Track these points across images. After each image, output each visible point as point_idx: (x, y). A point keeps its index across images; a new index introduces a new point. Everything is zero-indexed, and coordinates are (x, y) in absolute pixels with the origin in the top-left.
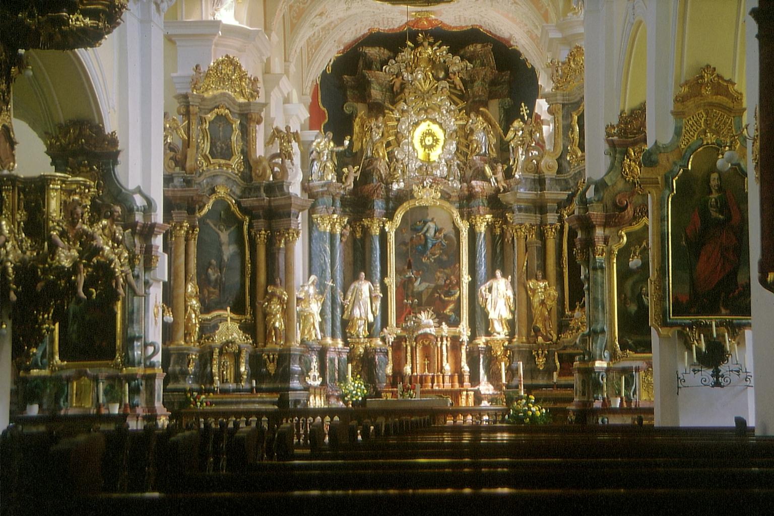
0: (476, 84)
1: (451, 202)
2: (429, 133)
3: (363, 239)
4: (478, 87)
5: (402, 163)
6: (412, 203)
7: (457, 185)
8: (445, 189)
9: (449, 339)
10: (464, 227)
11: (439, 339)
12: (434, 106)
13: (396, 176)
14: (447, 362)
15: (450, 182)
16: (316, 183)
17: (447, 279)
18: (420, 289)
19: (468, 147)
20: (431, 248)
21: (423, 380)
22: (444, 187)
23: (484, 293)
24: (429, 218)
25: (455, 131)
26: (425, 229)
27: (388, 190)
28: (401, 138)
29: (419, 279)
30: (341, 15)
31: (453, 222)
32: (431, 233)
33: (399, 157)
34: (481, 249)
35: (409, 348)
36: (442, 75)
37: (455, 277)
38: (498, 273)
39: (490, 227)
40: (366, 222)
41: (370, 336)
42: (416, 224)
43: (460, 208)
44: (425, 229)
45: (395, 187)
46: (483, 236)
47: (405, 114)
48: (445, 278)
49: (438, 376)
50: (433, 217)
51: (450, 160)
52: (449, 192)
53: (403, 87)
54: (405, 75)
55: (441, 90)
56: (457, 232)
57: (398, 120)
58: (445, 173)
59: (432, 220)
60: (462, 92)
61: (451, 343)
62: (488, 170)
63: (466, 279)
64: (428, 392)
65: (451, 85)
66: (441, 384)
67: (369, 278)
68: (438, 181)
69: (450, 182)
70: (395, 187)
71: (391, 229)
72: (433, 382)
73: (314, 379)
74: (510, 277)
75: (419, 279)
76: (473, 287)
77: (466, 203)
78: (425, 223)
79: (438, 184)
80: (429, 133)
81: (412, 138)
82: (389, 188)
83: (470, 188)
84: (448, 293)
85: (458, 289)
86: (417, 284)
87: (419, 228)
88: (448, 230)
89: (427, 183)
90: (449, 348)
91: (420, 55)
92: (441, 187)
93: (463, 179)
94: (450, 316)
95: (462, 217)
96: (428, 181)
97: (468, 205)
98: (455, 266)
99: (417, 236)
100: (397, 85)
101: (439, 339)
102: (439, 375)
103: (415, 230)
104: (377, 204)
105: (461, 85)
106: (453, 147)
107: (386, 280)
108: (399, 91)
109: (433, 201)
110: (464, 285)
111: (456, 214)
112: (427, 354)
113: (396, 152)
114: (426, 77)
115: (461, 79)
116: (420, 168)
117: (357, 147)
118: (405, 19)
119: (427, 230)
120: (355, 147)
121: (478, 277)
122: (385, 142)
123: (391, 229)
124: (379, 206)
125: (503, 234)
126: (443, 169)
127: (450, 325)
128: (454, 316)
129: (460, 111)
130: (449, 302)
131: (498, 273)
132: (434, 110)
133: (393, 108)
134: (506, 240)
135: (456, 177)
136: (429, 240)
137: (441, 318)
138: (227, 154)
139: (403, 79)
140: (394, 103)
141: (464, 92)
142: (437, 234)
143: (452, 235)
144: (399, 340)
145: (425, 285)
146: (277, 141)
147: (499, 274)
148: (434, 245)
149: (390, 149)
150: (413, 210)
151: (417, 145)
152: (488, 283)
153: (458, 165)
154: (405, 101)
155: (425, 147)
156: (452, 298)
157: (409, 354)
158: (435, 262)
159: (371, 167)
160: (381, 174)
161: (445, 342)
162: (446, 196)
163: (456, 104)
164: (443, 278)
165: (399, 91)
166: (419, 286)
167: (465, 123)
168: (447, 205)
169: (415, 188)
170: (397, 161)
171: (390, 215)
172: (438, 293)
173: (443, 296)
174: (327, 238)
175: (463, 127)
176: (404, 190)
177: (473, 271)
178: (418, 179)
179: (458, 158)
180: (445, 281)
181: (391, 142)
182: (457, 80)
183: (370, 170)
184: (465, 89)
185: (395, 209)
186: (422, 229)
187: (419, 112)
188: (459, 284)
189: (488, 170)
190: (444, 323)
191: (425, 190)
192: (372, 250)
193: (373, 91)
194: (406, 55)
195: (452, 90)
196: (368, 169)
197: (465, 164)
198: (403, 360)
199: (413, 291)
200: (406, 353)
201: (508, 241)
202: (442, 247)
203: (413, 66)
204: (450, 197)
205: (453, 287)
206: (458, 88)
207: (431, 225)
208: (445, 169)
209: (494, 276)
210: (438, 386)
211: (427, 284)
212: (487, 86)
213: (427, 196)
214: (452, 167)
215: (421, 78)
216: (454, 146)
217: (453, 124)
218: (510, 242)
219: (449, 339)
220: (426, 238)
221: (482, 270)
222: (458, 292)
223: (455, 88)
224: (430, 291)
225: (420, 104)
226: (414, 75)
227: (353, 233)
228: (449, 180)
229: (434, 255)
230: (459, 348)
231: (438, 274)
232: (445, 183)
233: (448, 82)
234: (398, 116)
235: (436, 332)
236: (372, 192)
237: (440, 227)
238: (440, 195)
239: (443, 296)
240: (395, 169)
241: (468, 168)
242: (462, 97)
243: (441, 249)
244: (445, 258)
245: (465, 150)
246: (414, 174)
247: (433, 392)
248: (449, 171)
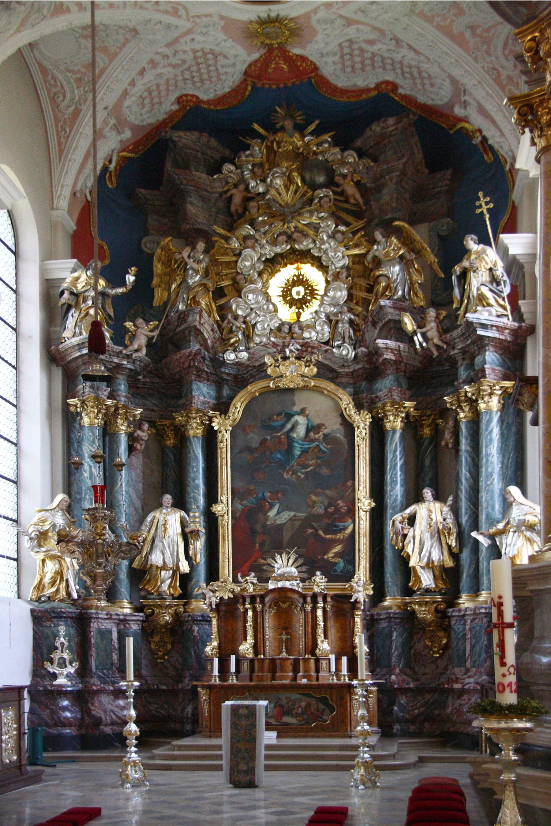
0: (385, 191)
1: (338, 384)
2: (299, 281)
4: (388, 194)
5: (244, 322)
6: (261, 384)
7: (347, 352)
8: (326, 362)
9: (329, 599)
11: (309, 599)
12: (305, 228)
13: (232, 341)
14: (326, 637)
15: (334, 350)
17: (330, 505)
18: (278, 522)
19: (370, 289)
20: (300, 456)
21: (274, 666)
22: (325, 358)
23: (399, 526)
24: (296, 408)
25: (347, 268)
26: (289, 426)
27: (218, 363)
28: (242, 282)
29: (277, 507)
31: (342, 415)
32: (301, 431)
33: (240, 312)
34: (395, 456)
35: (250, 613)
36: (321, 179)
37: (344, 502)
38: (428, 493)
42: (271, 419)
44: (289, 426)
46: (398, 435)
47: (249, 243)
48: (326, 504)
49: (306, 660)
50: (302, 406)
51: (336, 315)
52: (334, 366)
54: (252, 184)
55: (319, 202)
56: (349, 428)
57: (240, 254)
58: (327, 336)
59: (302, 412)
60: (360, 207)
61: (332, 606)
63: (364, 503)
64: (284, 687)
65: (338, 198)
66: (313, 674)
68: (313, 348)
69: (334, 350)
70: (230, 356)
71: (223, 426)
72: (296, 670)
73: (62, 664)
74: (451, 498)
75: (277, 507)
76: (378, 516)
77: (363, 378)
78: (289, 416)
79: (313, 353)
80: (299, 281)
81: (265, 285)
82: (218, 360)
84: (333, 529)
85: (350, 521)
86: (272, 513)
87: (276, 424)
88: (333, 426)
89: (291, 351)
90: (330, 614)
91: (279, 147)
94: (335, 564)
95: (359, 407)
96: (293, 348)
97: (371, 388)
98: (344, 484)
99: (272, 437)
100: (237, 199)
101: (309, 599)
102: (309, 659)
103: (267, 426)
104: (199, 389)
105: (358, 196)
106: (342, 295)
108: (240, 211)
109: (303, 380)
110: (362, 514)
111: (346, 402)
112: (285, 626)
113: (234, 307)
114: (290, 180)
115: (358, 184)
116: (279, 329)
117: (159, 296)
119: (293, 428)
120: (156, 298)
121: (389, 501)
122: (211, 286)
125: (437, 433)
126: (322, 329)
127: (331, 577)
128: (342, 564)
129: (354, 233)
130: (333, 543)
131: (428, 493)
132: (306, 236)
133: (229, 234)
134: (443, 443)
135: (347, 340)
136: (296, 444)
137: (310, 565)
139: (247, 189)
140: (231, 227)
141: (364, 208)
142: (312, 434)
143: (339, 435)
145: (286, 516)
147: (430, 494)
148: (304, 452)
149: (222, 301)
150: (267, 392)
151: (277, 300)
152: (408, 511)
153: (351, 322)
154: (252, 223)
155: (292, 303)
156: (339, 536)
157: (250, 623)
158: (306, 477)
159: (183, 327)
160: (205, 340)
161: (321, 604)
162: (327, 372)
163: (347, 224)
164: (322, 502)
165: (240, 211)
166: (276, 515)
167: (362, 252)
168: (331, 387)
169: (268, 360)
170: (236, 317)
172: (312, 527)
173: (321, 533)
175: (358, 259)
176: (248, 366)
177: (378, 490)
178: (275, 345)
179: (350, 310)
180: (326, 508)
181: (226, 291)
182: (351, 190)
183: (183, 331)
184: (365, 204)
186: (283, 426)
187: (276, 239)
188: (351, 512)
190: (318, 573)
191: (287, 362)
193: (190, 209)
194: (258, 151)
195: (340, 204)
196: (178, 330)
197: (365, 318)
198: (241, 632)
199: (264, 526)
200: (245, 621)
201: (447, 445)
202: (320, 455)
203: (267, 166)
204: (337, 377)
205: (342, 518)
206: (352, 201)
207: (300, 419)
208: (327, 329)
209: (418, 499)
210: (309, 677)
211: (292, 514)
212: (407, 196)
213: (292, 372)
214: (340, 325)
215: (279, 186)
216: (345, 293)
217: (339, 258)
218: (450, 446)
219: (329, 599)
220: (290, 441)
221: (396, 490)
222: (351, 527)
223: (347, 201)
224: (297, 524)
225: (278, 226)
226: (269, 180)
228: (333, 347)
229: (305, 466)
230: (349, 615)
231: (314, 498)
232: (326, 351)
233: (334, 193)
234: (235, 244)
235: (304, 589)
236: (186, 365)
237: (316, 421)
238: (315, 370)
239: (321, 533)
240: (231, 331)
241: (370, 324)
242: (358, 215)
243: (318, 458)
244: (325, 471)
245: (363, 295)
246: (269, 339)
247: (295, 687)
248: (333, 332)
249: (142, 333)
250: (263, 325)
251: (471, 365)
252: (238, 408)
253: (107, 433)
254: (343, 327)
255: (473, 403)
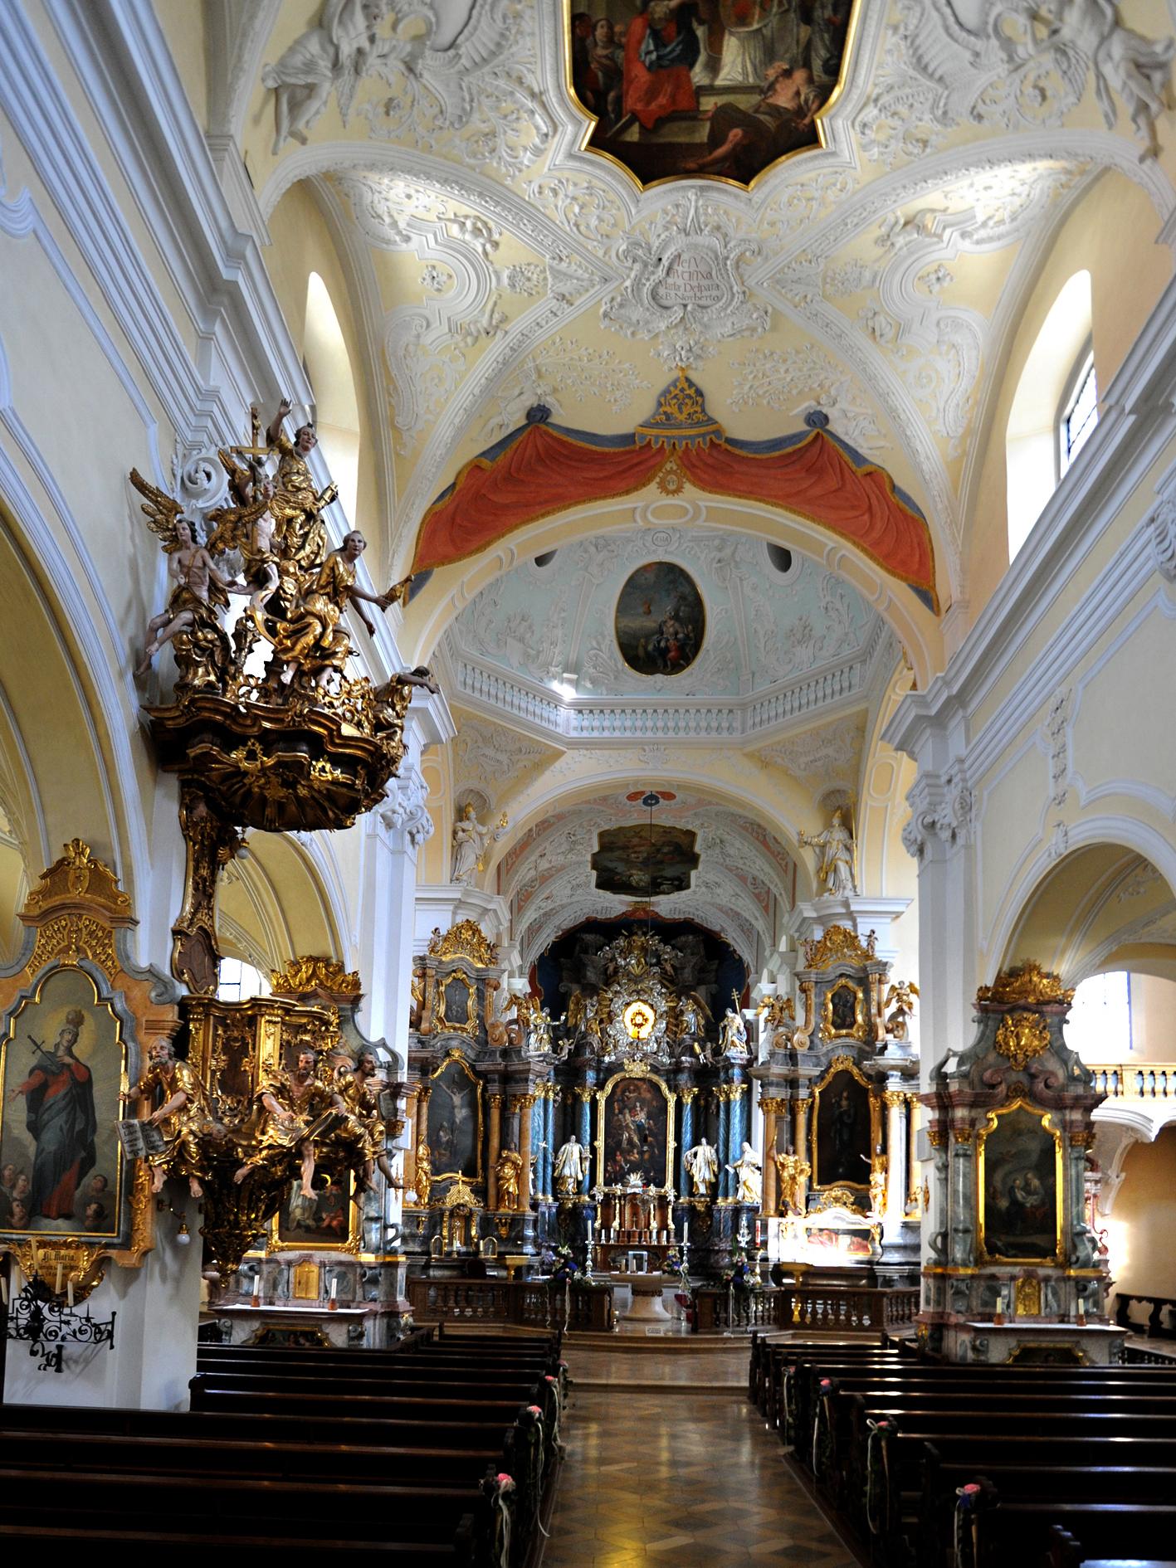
3: (573, 1106)
7: (666, 1060)
10: (672, 1099)
16: (533, 1053)
27: (600, 1062)
30: (565, 901)
39: (696, 1099)
40: (578, 1090)
41: (579, 1193)
43: (667, 1082)
45: (607, 1059)
53: (616, 971)
62: (696, 1046)
67: (578, 1141)
70: (607, 1059)
83: (679, 1063)
92: (650, 1061)
93: (671, 1055)
96: (639, 1055)
107: (596, 1144)
118: (624, 909)
123: (601, 1097)
124: (591, 1076)
138: (463, 1018)
144: (608, 1197)
146: (515, 1008)
162: (655, 1069)
171: (601, 1085)
174: (540, 1102)
185: (605, 1080)
189: (696, 1046)
192: (581, 1116)
227: (564, 1099)
249: (567, 1045)
250: (623, 1040)
251: (727, 1072)
252: (609, 1088)
253: (546, 1101)
254: (664, 1046)
255: (728, 1096)
